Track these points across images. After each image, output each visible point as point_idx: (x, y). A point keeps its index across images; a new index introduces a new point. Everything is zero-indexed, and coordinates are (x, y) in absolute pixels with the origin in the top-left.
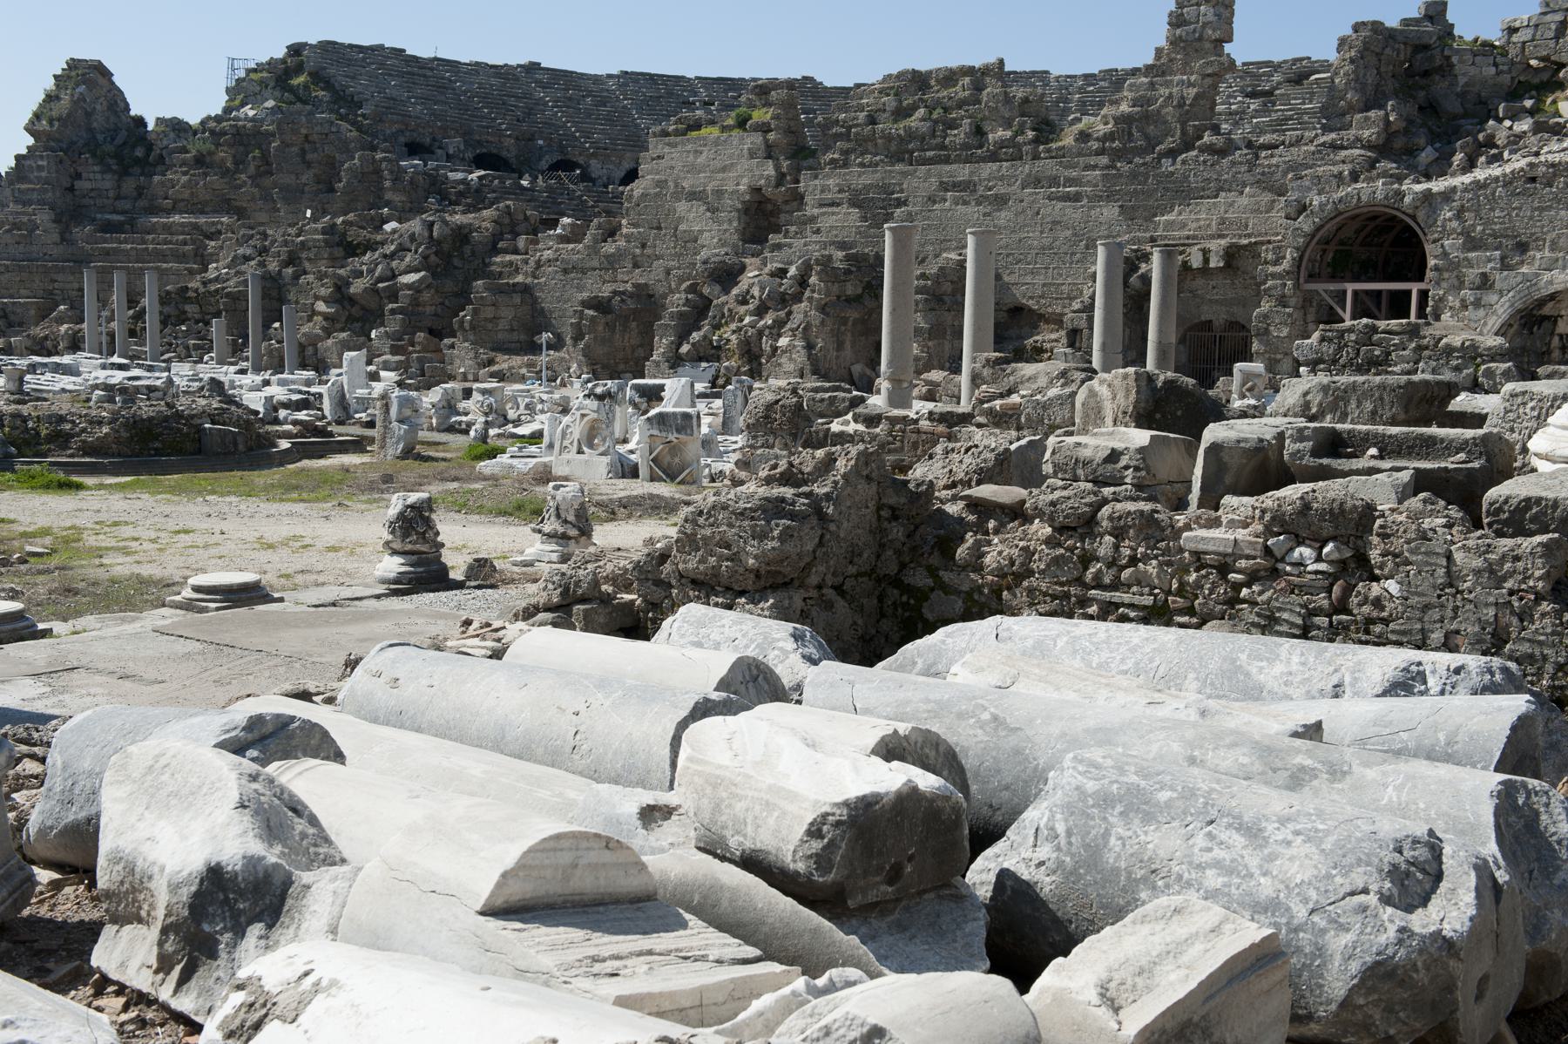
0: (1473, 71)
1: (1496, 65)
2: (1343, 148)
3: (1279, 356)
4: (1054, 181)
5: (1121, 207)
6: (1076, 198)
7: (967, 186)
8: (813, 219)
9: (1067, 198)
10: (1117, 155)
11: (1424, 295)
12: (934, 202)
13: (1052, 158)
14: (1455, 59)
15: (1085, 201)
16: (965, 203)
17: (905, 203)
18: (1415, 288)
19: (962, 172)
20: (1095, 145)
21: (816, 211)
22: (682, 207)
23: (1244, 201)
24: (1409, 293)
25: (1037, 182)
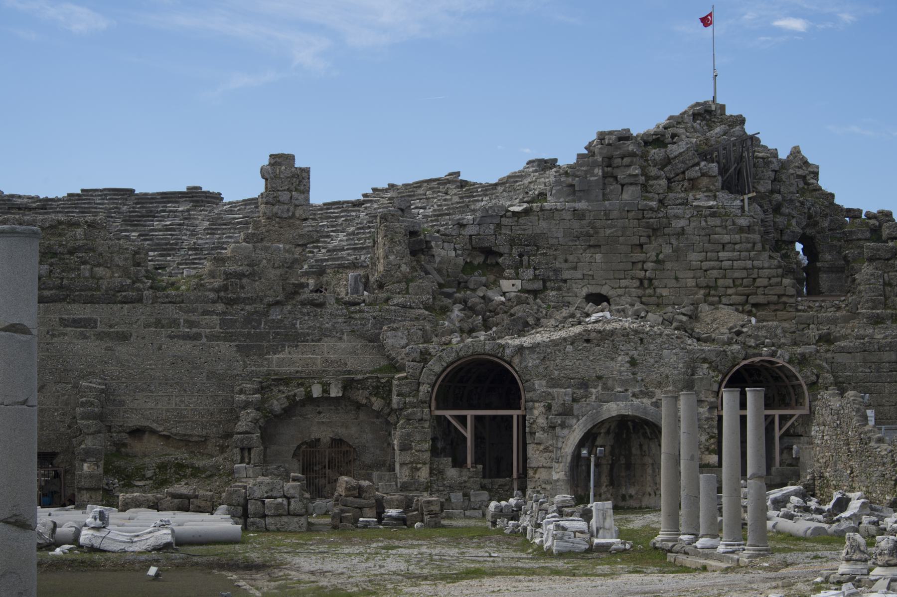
0: (443, 253)
1: (455, 249)
2: (411, 307)
3: (419, 466)
5: (236, 346)
6: (197, 337)
7: (89, 323)
9: (187, 337)
10: (230, 302)
12: (53, 336)
13: (170, 302)
14: (433, 244)
15: (204, 340)
16: (86, 337)
18: (515, 413)
20: (212, 295)
23: (341, 345)
24: (512, 416)
25: (158, 324)
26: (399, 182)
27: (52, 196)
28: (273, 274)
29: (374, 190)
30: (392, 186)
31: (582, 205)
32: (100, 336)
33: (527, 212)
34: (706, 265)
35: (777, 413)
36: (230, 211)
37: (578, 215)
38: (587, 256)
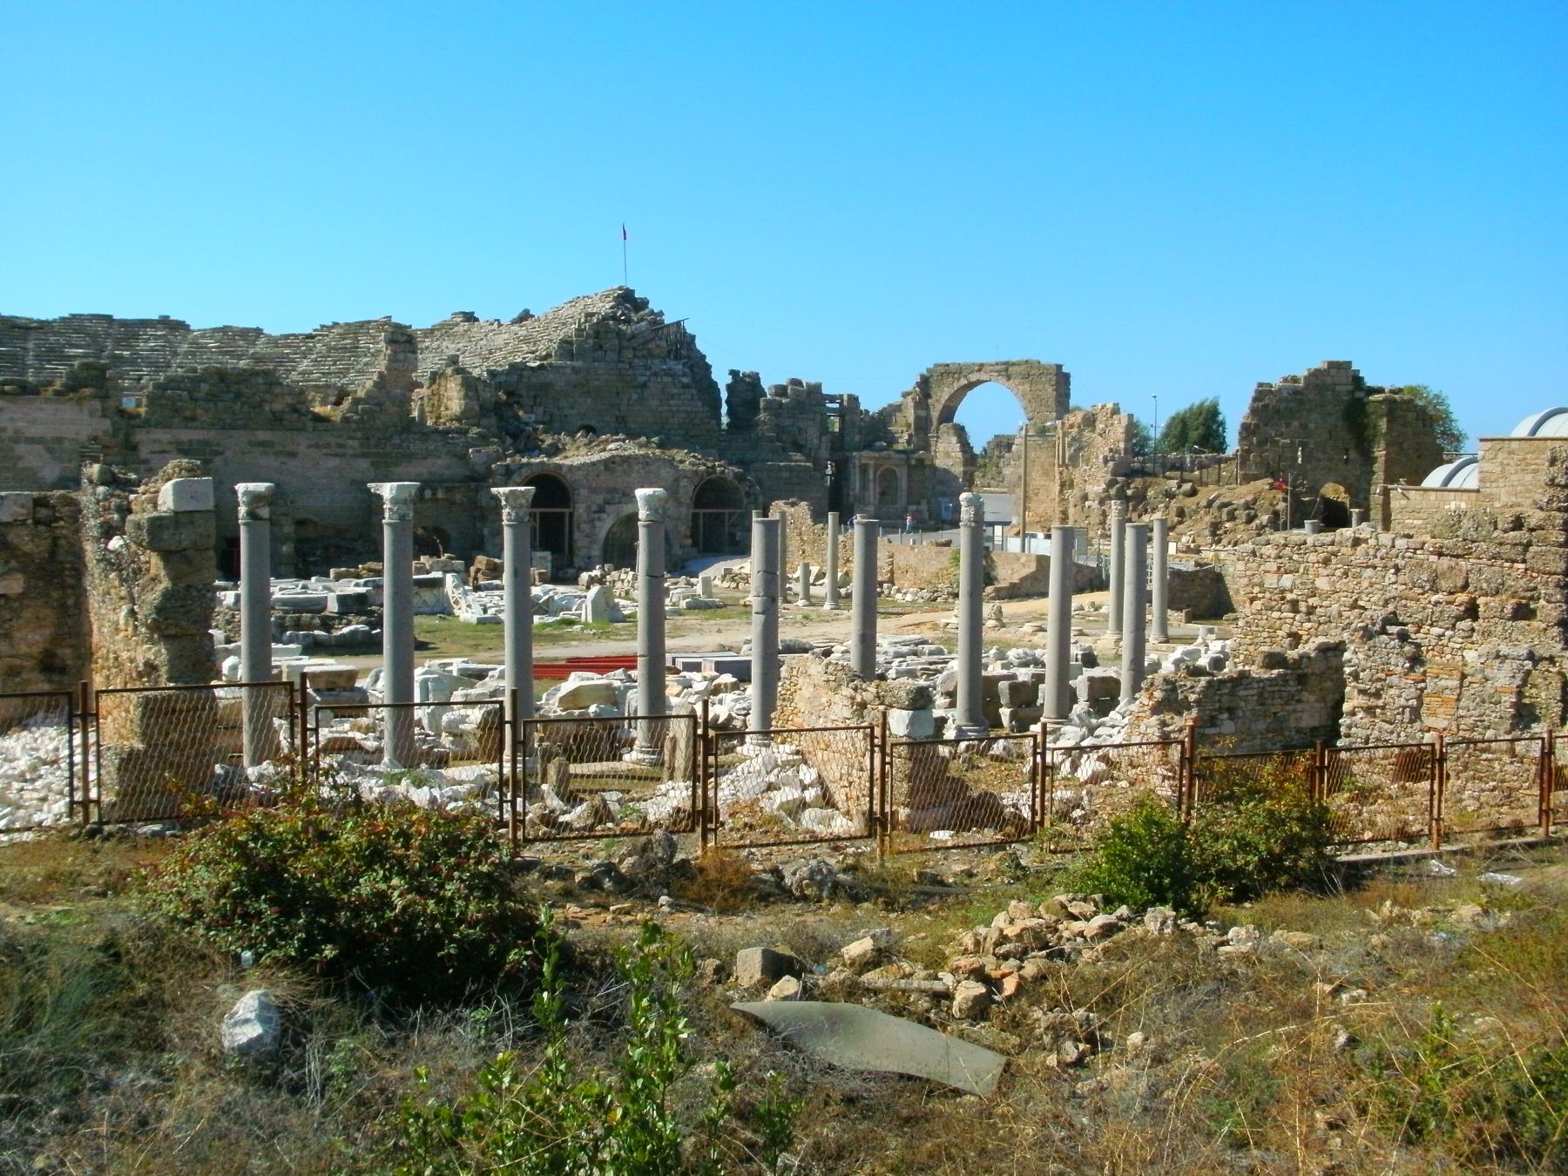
4: (328, 445)
6: (343, 455)
8: (146, 461)
9: (336, 455)
11: (571, 515)
17: (222, 453)
18: (566, 511)
19: (263, 435)
20: (353, 426)
21: (149, 457)
22: (21, 449)
25: (317, 446)
26: (341, 321)
27: (43, 318)
28: (394, 410)
29: (323, 326)
30: (336, 324)
31: (578, 364)
32: (277, 454)
33: (541, 367)
34: (661, 409)
35: (702, 511)
36: (203, 336)
37: (575, 371)
38: (582, 400)
